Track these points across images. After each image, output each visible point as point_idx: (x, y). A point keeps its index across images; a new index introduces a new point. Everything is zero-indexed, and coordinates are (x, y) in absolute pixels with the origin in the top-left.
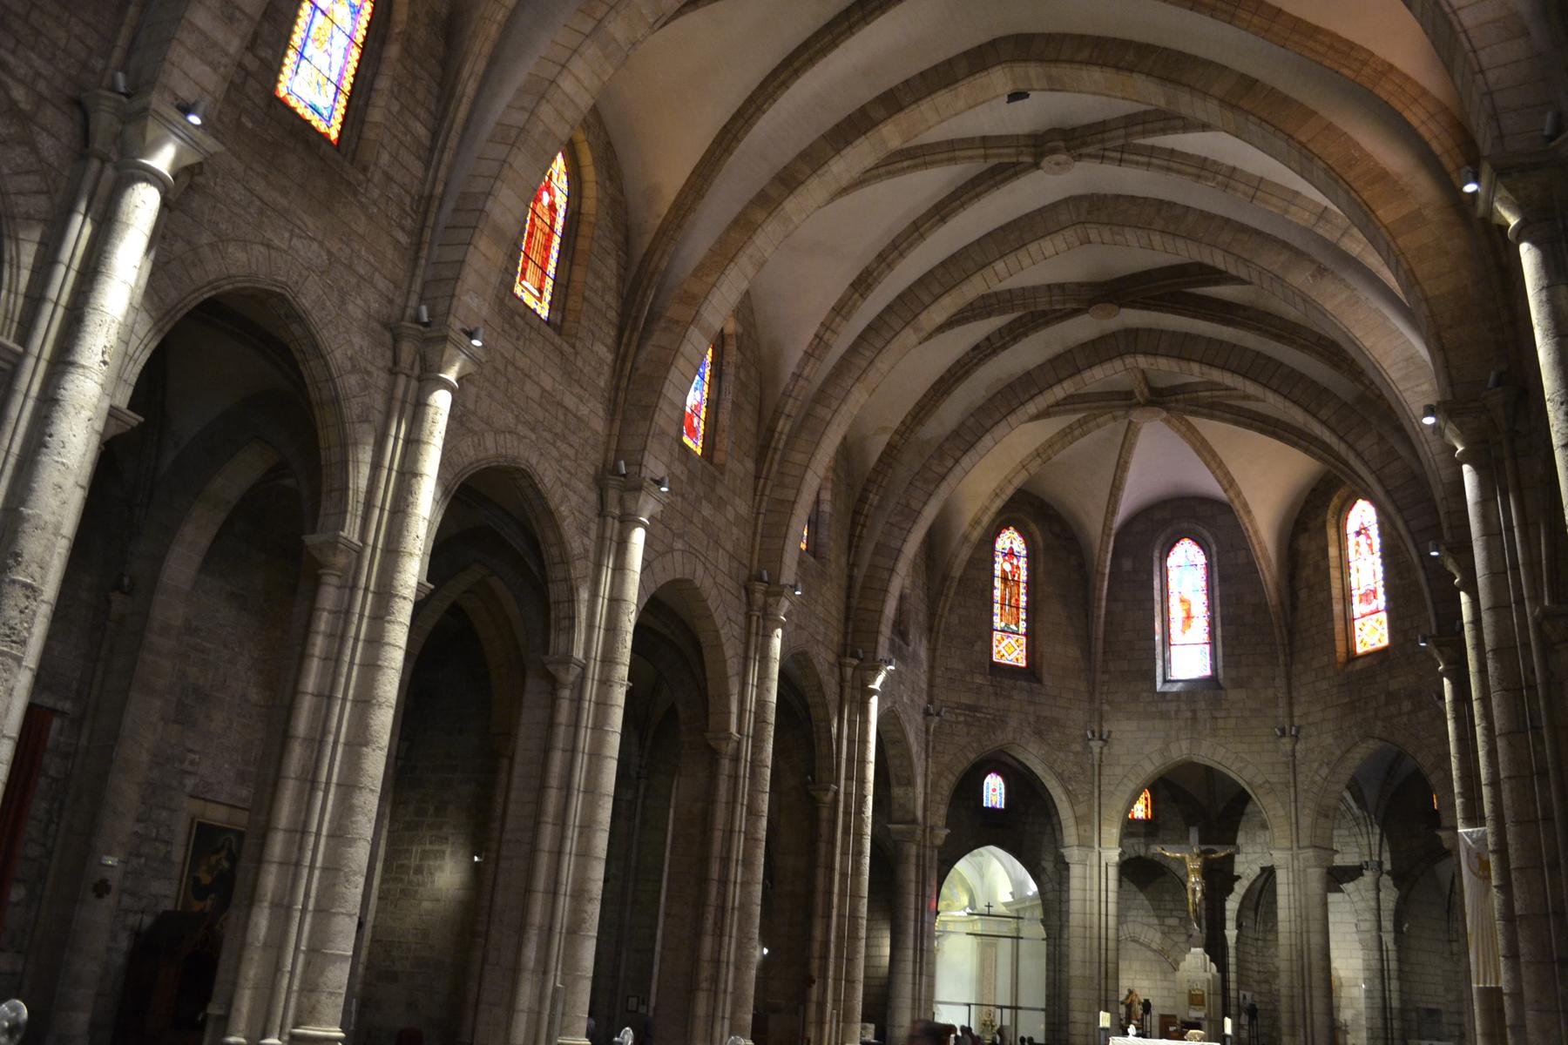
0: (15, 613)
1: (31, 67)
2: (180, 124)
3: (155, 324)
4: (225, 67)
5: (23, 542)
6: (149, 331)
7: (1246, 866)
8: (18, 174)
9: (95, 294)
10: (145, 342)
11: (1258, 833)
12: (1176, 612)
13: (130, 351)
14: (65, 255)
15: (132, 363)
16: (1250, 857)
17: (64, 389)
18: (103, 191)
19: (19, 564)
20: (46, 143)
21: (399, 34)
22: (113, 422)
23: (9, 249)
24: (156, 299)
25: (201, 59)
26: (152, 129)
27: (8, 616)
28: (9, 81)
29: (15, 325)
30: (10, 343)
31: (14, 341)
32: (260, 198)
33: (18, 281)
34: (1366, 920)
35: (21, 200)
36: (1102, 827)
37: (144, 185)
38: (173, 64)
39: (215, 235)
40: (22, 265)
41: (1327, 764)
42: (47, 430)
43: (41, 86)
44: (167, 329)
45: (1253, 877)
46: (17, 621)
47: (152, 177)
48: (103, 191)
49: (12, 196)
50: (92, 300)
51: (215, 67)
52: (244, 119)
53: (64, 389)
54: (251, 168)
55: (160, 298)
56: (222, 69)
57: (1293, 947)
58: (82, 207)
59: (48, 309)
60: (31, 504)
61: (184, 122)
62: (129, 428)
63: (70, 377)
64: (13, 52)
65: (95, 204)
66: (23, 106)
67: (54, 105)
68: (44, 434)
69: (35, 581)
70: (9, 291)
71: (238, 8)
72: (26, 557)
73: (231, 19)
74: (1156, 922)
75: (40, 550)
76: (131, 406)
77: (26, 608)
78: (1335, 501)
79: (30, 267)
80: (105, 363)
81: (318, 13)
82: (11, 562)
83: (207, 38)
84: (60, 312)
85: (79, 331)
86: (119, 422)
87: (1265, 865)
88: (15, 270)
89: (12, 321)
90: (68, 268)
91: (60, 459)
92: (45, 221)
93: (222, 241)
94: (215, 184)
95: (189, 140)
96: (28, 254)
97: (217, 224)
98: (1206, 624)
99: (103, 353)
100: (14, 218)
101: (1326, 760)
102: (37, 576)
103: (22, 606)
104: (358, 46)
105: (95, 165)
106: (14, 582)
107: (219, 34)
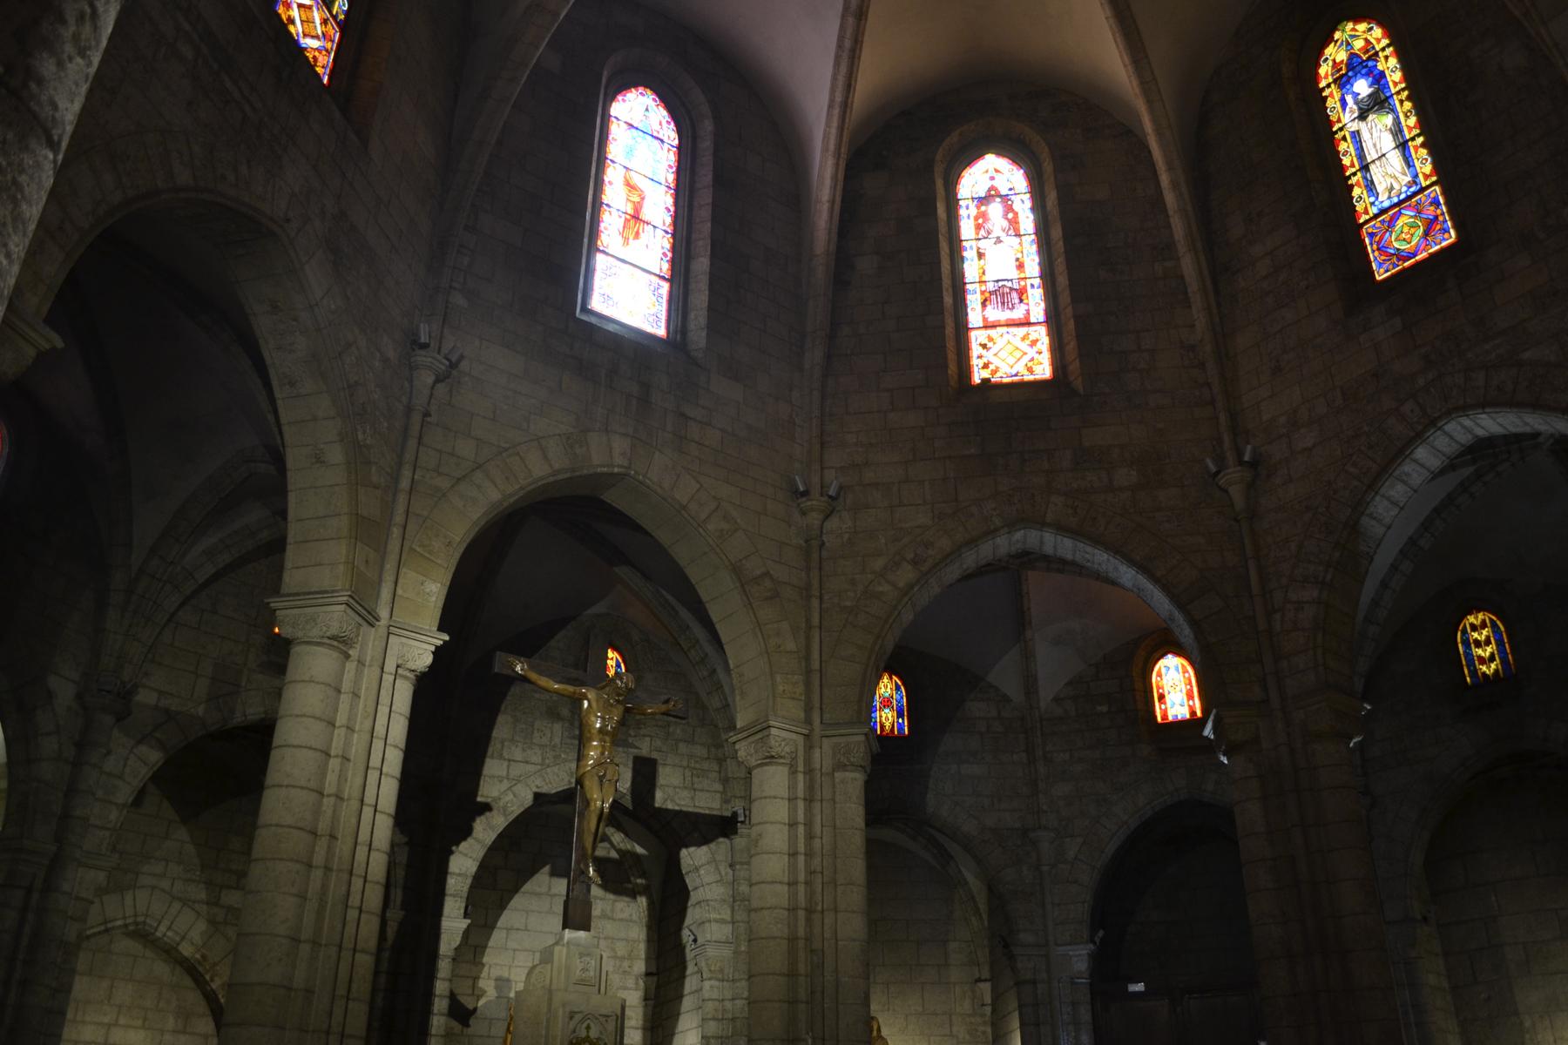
7: (506, 784)
11: (537, 724)
12: (614, 195)
16: (517, 770)
34: (722, 921)
36: (403, 570)
41: (915, 562)
45: (516, 810)
57: (801, 944)
74: (203, 896)
78: (954, 138)
87: (545, 789)
98: (668, 246)
101: (910, 556)
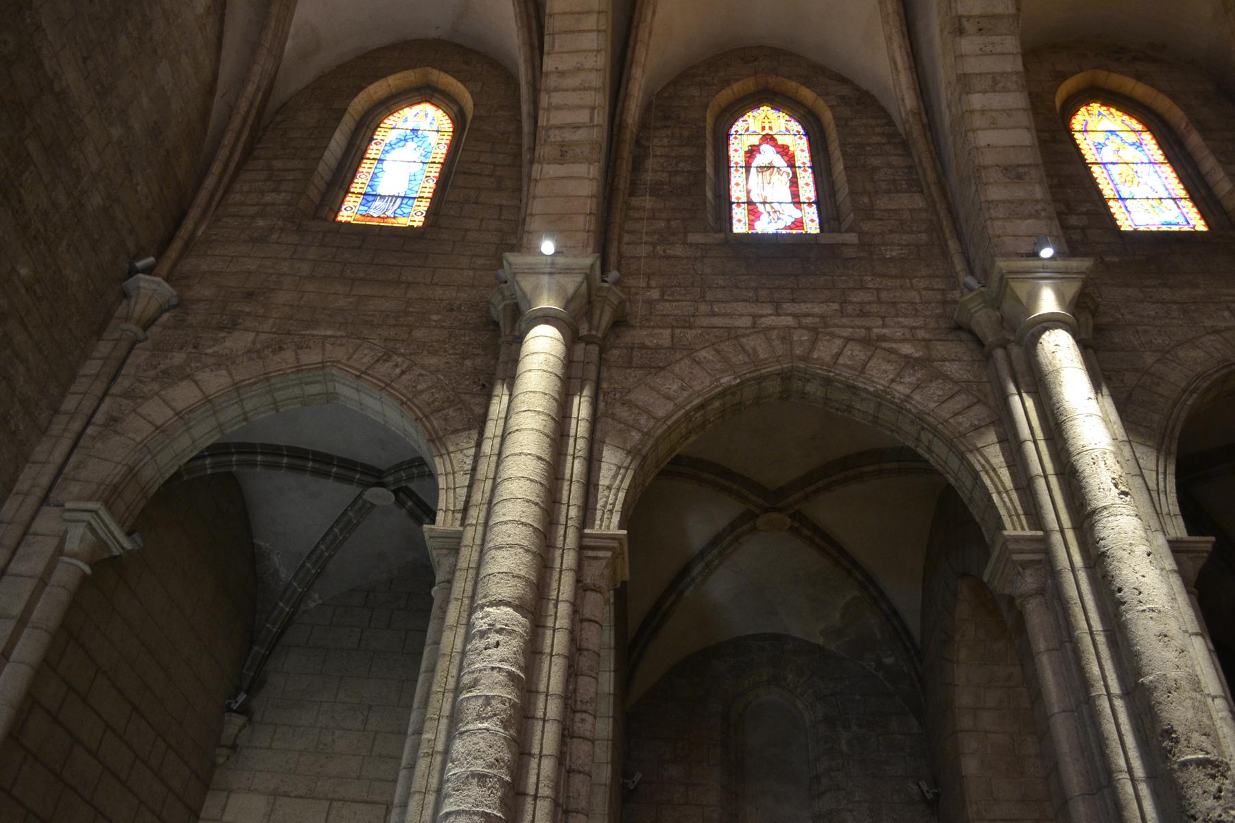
0: (1210, 802)
1: (903, 327)
2: (1038, 268)
3: (1159, 451)
4: (1044, 210)
5: (1164, 714)
6: (1158, 460)
8: (943, 402)
9: (1071, 441)
10: (1161, 470)
13: (1152, 485)
14: (1025, 432)
15: (1162, 496)
17: (1102, 539)
18: (1020, 367)
19: (1177, 741)
20: (952, 368)
21: (1187, 125)
22: (1184, 557)
23: (976, 461)
24: (1142, 430)
25: (1020, 219)
26: (1021, 289)
27: (1203, 809)
28: (894, 345)
29: (1023, 518)
30: (1028, 533)
31: (1031, 529)
32: (1174, 302)
33: (1002, 482)
35: (960, 419)
37: (1047, 333)
38: (999, 236)
39: (1156, 351)
40: (995, 466)
42: (1113, 588)
43: (921, 334)
44: (1174, 448)
46: (1219, 811)
47: (1051, 322)
48: (1020, 367)
49: (951, 420)
50: (1072, 449)
51: (1036, 215)
52: (1107, 259)
53: (1102, 539)
54: (1146, 286)
55: (1146, 427)
56: (1043, 214)
58: (1012, 388)
59: (1041, 484)
60: (1146, 669)
61: (1040, 263)
62: (1206, 555)
63: (1100, 526)
64: (884, 326)
65: (1020, 380)
66: (917, 355)
67: (940, 340)
68: (1113, 593)
69: (1208, 753)
70: (999, 493)
71: (1019, 166)
72: (1180, 729)
73: (1019, 177)
75: (1190, 714)
76: (1190, 533)
77: (1220, 790)
79: (1004, 464)
80: (1126, 494)
81: (1109, 166)
82: (1167, 744)
83: (1011, 202)
84: (1053, 480)
85: (1079, 481)
86: (1191, 555)
88: (992, 474)
89: (1018, 516)
90: (1035, 442)
91: (1144, 607)
92: (992, 423)
93: (1168, 352)
94: (1122, 315)
95: (1058, 276)
96: (995, 455)
97: (1151, 342)
99: (1116, 485)
100: (964, 436)
102: (1207, 745)
103: (1214, 789)
104: (1162, 163)
105: (999, 353)
106: (1185, 764)
107: (1019, 192)
